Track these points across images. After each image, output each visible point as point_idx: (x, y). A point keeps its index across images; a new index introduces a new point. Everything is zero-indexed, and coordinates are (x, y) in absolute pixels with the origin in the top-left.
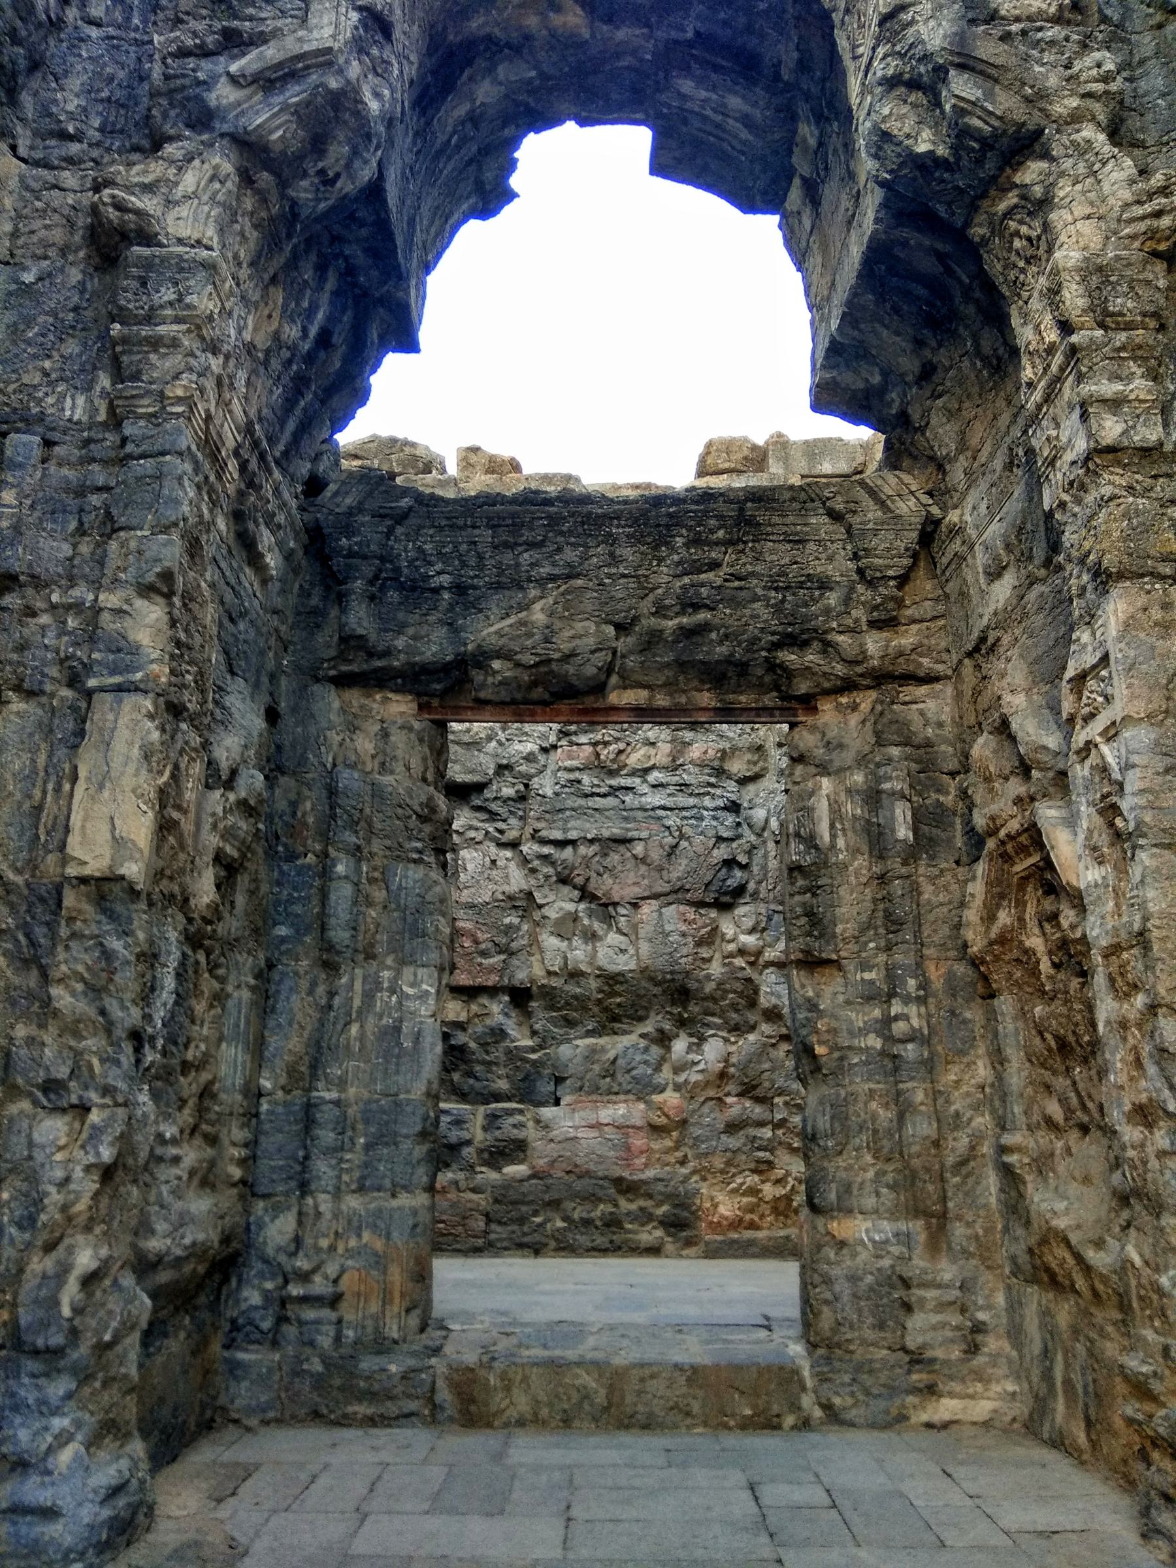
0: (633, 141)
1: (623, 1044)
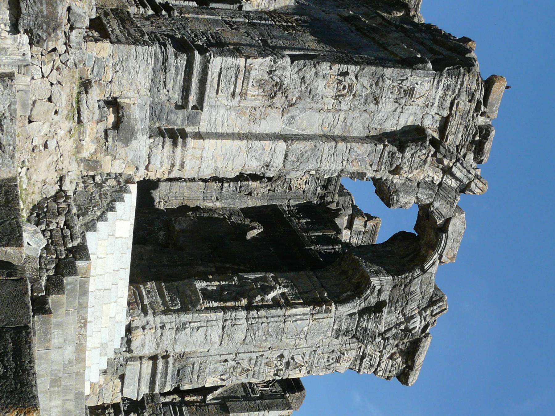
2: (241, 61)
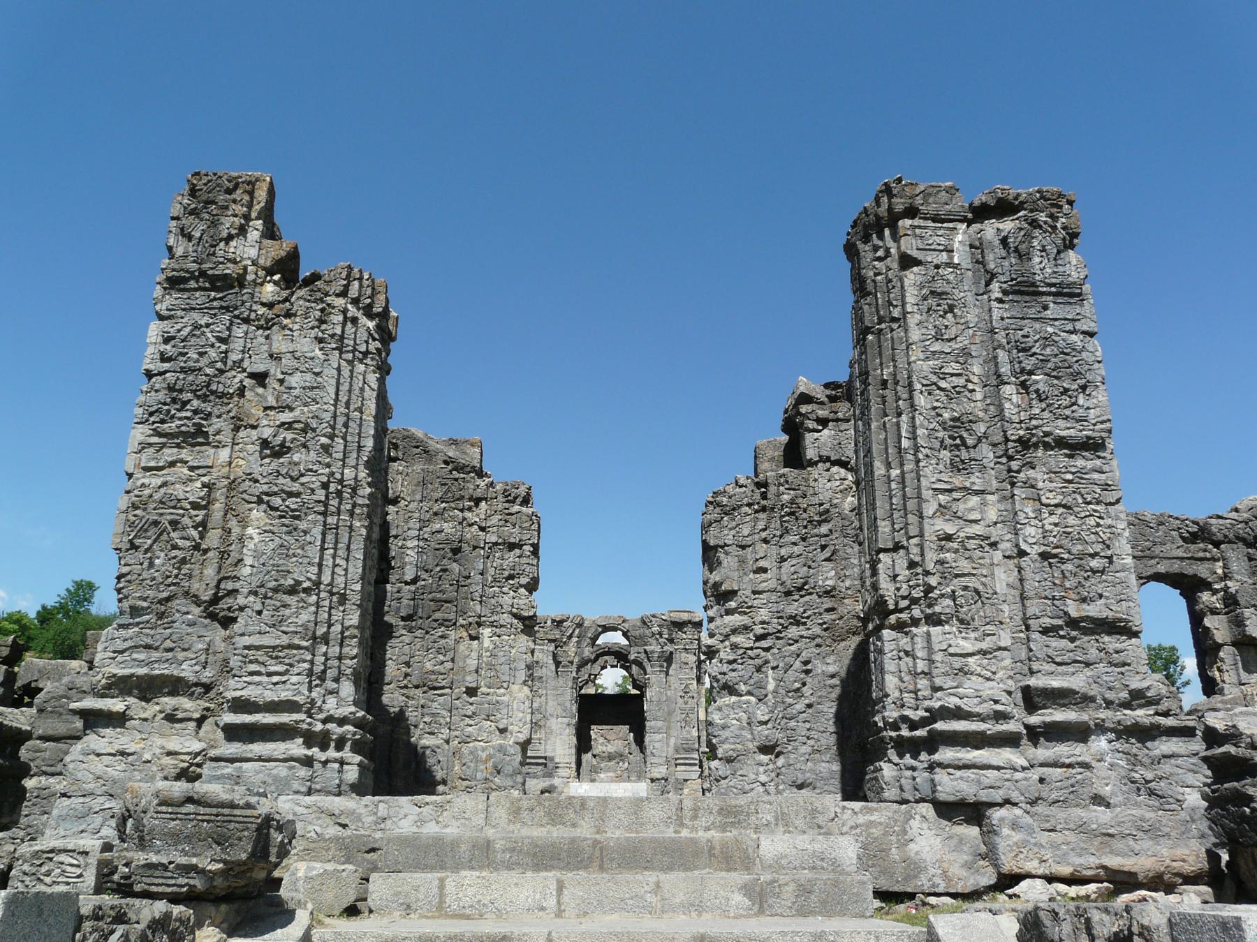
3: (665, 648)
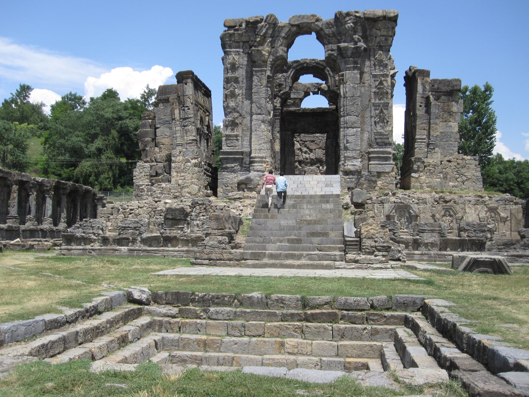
0: (312, 75)
1: (314, 167)
2: (224, 139)
3: (359, 44)
